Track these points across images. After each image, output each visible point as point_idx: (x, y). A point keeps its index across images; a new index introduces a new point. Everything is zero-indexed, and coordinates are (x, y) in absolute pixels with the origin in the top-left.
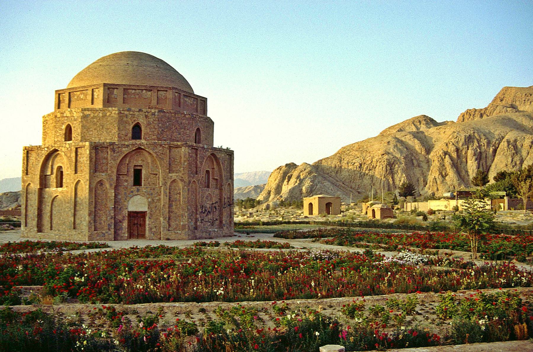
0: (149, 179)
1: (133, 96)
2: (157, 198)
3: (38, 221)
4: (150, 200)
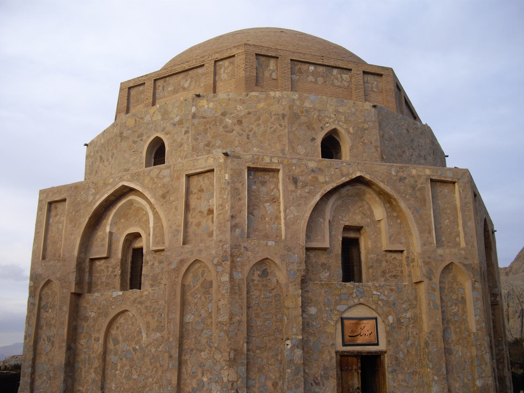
0: (384, 264)
1: (311, 78)
2: (409, 315)
3: (65, 381)
4: (391, 319)
